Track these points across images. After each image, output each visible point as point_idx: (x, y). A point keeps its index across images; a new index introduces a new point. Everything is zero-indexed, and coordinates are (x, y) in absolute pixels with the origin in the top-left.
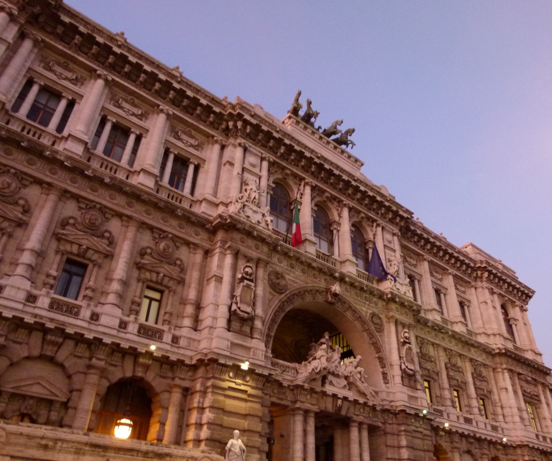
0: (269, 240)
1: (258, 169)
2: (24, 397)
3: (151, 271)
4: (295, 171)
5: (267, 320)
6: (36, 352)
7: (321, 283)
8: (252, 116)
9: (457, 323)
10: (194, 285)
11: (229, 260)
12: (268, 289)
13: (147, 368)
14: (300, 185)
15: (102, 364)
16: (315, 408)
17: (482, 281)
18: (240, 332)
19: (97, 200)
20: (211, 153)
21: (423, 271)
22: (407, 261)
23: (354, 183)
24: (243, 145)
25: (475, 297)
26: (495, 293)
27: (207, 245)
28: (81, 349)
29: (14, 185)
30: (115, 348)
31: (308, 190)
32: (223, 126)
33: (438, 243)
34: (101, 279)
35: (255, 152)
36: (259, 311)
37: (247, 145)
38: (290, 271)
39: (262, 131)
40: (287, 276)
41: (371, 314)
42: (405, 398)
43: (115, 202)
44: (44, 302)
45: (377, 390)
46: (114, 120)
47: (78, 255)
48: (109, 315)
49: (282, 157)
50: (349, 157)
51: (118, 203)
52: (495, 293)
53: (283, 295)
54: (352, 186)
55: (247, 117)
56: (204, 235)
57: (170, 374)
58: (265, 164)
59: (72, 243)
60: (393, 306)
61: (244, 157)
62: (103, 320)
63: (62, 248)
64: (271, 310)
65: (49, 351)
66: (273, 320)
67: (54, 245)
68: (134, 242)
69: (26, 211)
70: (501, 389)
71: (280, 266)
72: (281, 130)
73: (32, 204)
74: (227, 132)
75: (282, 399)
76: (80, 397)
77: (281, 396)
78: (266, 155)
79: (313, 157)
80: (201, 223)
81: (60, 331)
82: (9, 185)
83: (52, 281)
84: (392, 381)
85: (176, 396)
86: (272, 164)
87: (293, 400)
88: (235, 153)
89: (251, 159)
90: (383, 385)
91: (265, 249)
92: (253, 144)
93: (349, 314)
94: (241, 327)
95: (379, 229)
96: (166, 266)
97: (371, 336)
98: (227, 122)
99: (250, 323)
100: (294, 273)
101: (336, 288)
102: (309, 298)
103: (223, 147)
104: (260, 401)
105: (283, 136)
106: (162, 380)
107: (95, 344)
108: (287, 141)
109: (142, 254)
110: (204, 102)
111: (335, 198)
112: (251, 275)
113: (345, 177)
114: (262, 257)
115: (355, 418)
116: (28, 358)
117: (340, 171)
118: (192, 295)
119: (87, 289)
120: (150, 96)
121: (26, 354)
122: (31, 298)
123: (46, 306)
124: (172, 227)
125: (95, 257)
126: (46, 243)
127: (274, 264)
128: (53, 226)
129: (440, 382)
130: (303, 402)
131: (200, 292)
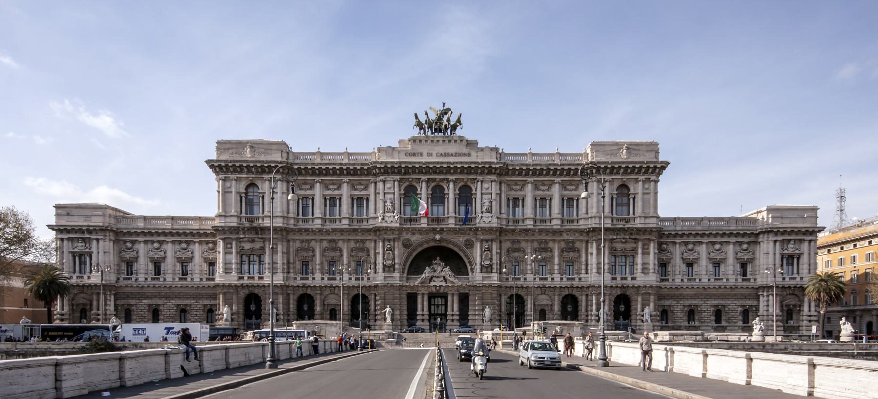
7: (431, 236)
10: (372, 256)
11: (381, 244)
18: (389, 272)
27: (374, 238)
30: (349, 287)
31: (424, 185)
36: (396, 261)
49: (405, 174)
50: (456, 141)
58: (396, 183)
66: (406, 262)
69: (313, 251)
71: (413, 231)
74: (375, 175)
85: (373, 297)
86: (400, 181)
88: (380, 185)
89: (388, 185)
93: (451, 246)
95: (479, 183)
97: (464, 253)
101: (438, 237)
102: (425, 246)
103: (376, 183)
109: (352, 251)
118: (372, 261)
122: (323, 279)
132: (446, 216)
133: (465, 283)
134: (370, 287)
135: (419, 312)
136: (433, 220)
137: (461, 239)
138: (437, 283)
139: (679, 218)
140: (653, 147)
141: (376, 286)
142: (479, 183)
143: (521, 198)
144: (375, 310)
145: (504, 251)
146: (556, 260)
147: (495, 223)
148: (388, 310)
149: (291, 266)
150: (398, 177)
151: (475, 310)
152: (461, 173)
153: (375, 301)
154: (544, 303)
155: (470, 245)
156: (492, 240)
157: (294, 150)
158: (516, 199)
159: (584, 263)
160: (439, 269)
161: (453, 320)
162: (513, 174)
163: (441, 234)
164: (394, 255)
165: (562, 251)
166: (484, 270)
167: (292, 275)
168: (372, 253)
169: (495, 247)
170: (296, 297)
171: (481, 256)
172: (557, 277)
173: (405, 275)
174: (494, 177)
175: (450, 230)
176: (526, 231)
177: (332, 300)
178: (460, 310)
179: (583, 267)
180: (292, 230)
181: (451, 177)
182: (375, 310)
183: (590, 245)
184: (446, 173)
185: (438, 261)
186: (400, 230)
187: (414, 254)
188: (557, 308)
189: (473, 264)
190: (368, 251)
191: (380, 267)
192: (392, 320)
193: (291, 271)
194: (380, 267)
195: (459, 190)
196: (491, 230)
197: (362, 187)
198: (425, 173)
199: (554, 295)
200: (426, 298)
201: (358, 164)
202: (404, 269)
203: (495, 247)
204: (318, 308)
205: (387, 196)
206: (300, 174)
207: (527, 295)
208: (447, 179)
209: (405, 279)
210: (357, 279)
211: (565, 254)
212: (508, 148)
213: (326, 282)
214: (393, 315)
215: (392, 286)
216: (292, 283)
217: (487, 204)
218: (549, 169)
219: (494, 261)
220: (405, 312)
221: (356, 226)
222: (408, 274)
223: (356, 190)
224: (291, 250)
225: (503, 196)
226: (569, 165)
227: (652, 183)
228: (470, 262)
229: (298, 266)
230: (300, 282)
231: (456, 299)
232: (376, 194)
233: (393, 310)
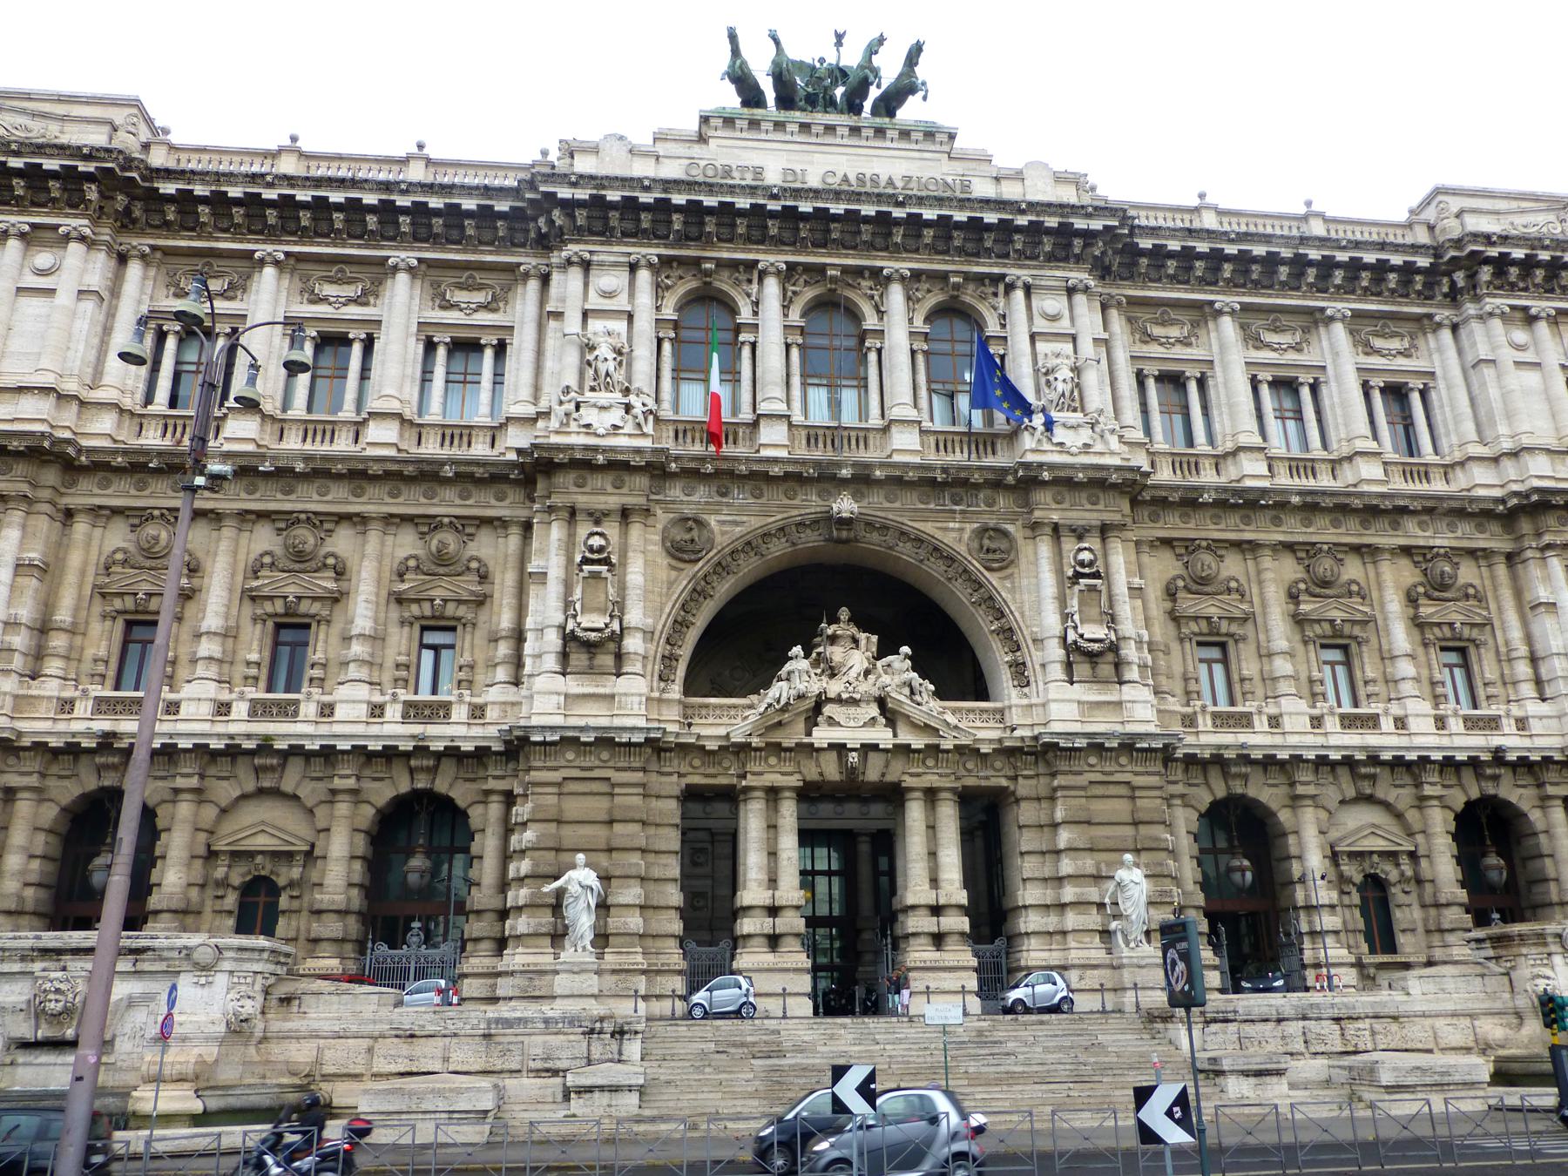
0: (637, 461)
1: (624, 297)
2: (251, 855)
3: (418, 601)
4: (725, 255)
5: (660, 627)
6: (250, 786)
7: (810, 503)
8: (574, 185)
9: (1350, 459)
11: (557, 532)
12: (664, 561)
13: (433, 771)
14: (750, 281)
15: (351, 783)
16: (794, 781)
17: (1477, 299)
18: (591, 671)
19: (299, 507)
20: (523, 306)
21: (1215, 348)
22: (1154, 339)
23: (898, 213)
24: (575, 259)
25: (1452, 353)
26: (1536, 318)
27: (522, 513)
28: (317, 768)
29: (164, 535)
31: (772, 287)
32: (533, 235)
33: (1259, 250)
34: (334, 639)
35: (612, 259)
36: (635, 615)
37: (587, 256)
38: (719, 503)
39: (613, 206)
40: (712, 520)
41: (973, 531)
42: (1072, 711)
43: (329, 498)
44: (240, 710)
45: (999, 705)
46: (314, 334)
47: (286, 615)
48: (347, 701)
49: (684, 239)
50: (905, 134)
51: (338, 498)
52: (1536, 318)
53: (700, 564)
54: (897, 222)
55: (564, 193)
56: (514, 495)
58: (644, 276)
59: (271, 598)
60: (1043, 497)
61: (586, 285)
62: (340, 712)
63: (259, 612)
64: (670, 604)
65: (266, 783)
66: (680, 625)
67: (248, 610)
68: (380, 559)
70: (1532, 608)
72: (654, 180)
73: (200, 555)
74: (545, 243)
75: (714, 776)
76: (328, 839)
77: (711, 771)
78: (639, 251)
79: (761, 202)
80: (493, 477)
81: (265, 746)
82: (156, 539)
83: (253, 671)
84: (1040, 678)
85: (495, 809)
87: (741, 772)
88: (567, 285)
90: (1014, 693)
91: (642, 481)
92: (602, 243)
93: (905, 552)
94: (590, 659)
95: (1019, 295)
96: (445, 582)
98: (535, 220)
99: (612, 646)
100: (728, 505)
101: (845, 505)
103: (545, 280)
104: (641, 790)
105: (665, 191)
106: (468, 785)
107: (328, 754)
108: (679, 199)
110: (469, 204)
111: (859, 272)
112: (601, 549)
113: (868, 210)
114: (630, 501)
115: (909, 781)
116: (244, 797)
117: (849, 201)
118: (506, 621)
119: (312, 666)
120: (367, 247)
121: (237, 793)
122: (223, 708)
123: (245, 716)
124: (448, 504)
125: (315, 608)
126: (234, 611)
127: (673, 502)
128: (240, 578)
129: (1262, 637)
130: (761, 774)
131: (521, 610)
132: (875, 421)
133: (986, 733)
134: (481, 754)
135: (752, 893)
136: (813, 435)
137: (954, 532)
138: (852, 728)
141: (517, 747)
142: (1019, 295)
143: (1192, 372)
144: (504, 886)
145: (1155, 593)
146: (1400, 637)
147: (1112, 454)
148: (581, 878)
149: (58, 642)
150: (653, 252)
151: (1060, 880)
152: (934, 250)
153: (508, 830)
154: (1379, 844)
155: (998, 550)
156: (1105, 530)
157: (175, 138)
158: (1173, 380)
159: (1523, 650)
160: (858, 660)
161: (938, 939)
162: (1156, 274)
163: (857, 496)
164: (622, 588)
165: (1412, 600)
166: (1082, 670)
167: (50, 688)
168: (504, 581)
169: (1119, 560)
170: (50, 813)
171: (1062, 600)
172: (1419, 711)
173: (676, 691)
174: (1078, 276)
175: (899, 481)
176: (1247, 503)
177: (264, 827)
178: (969, 882)
179: (1523, 669)
180: (101, 467)
181: (889, 265)
182: (504, 886)
183: (1534, 571)
184: (871, 246)
185: (844, 629)
186: (657, 470)
187: (724, 589)
188: (1445, 868)
189: (1024, 635)
190: (484, 577)
191: (543, 646)
192: (602, 939)
193: (53, 666)
194: (543, 646)
195: (928, 319)
196: (1098, 483)
197: (480, 297)
198: (778, 243)
199: (1421, 801)
200: (789, 812)
201: (469, 190)
202: (669, 660)
203: (1119, 560)
204: (173, 878)
205: (595, 325)
206: (189, 223)
207: (1295, 801)
208: (876, 273)
209: (674, 713)
210: (413, 711)
211: (1427, 610)
212: (1115, 187)
213: (240, 725)
214: (603, 907)
215: (605, 741)
216: (39, 726)
217: (1065, 373)
218: (1300, 263)
219: (1128, 627)
220: (674, 896)
221: (432, 448)
222: (687, 691)
223: (449, 306)
224: (75, 559)
225: (1121, 356)
226: (1382, 246)
228: (1008, 634)
229: (102, 640)
230: (85, 724)
231: (948, 815)
232: (548, 315)
233: (605, 878)
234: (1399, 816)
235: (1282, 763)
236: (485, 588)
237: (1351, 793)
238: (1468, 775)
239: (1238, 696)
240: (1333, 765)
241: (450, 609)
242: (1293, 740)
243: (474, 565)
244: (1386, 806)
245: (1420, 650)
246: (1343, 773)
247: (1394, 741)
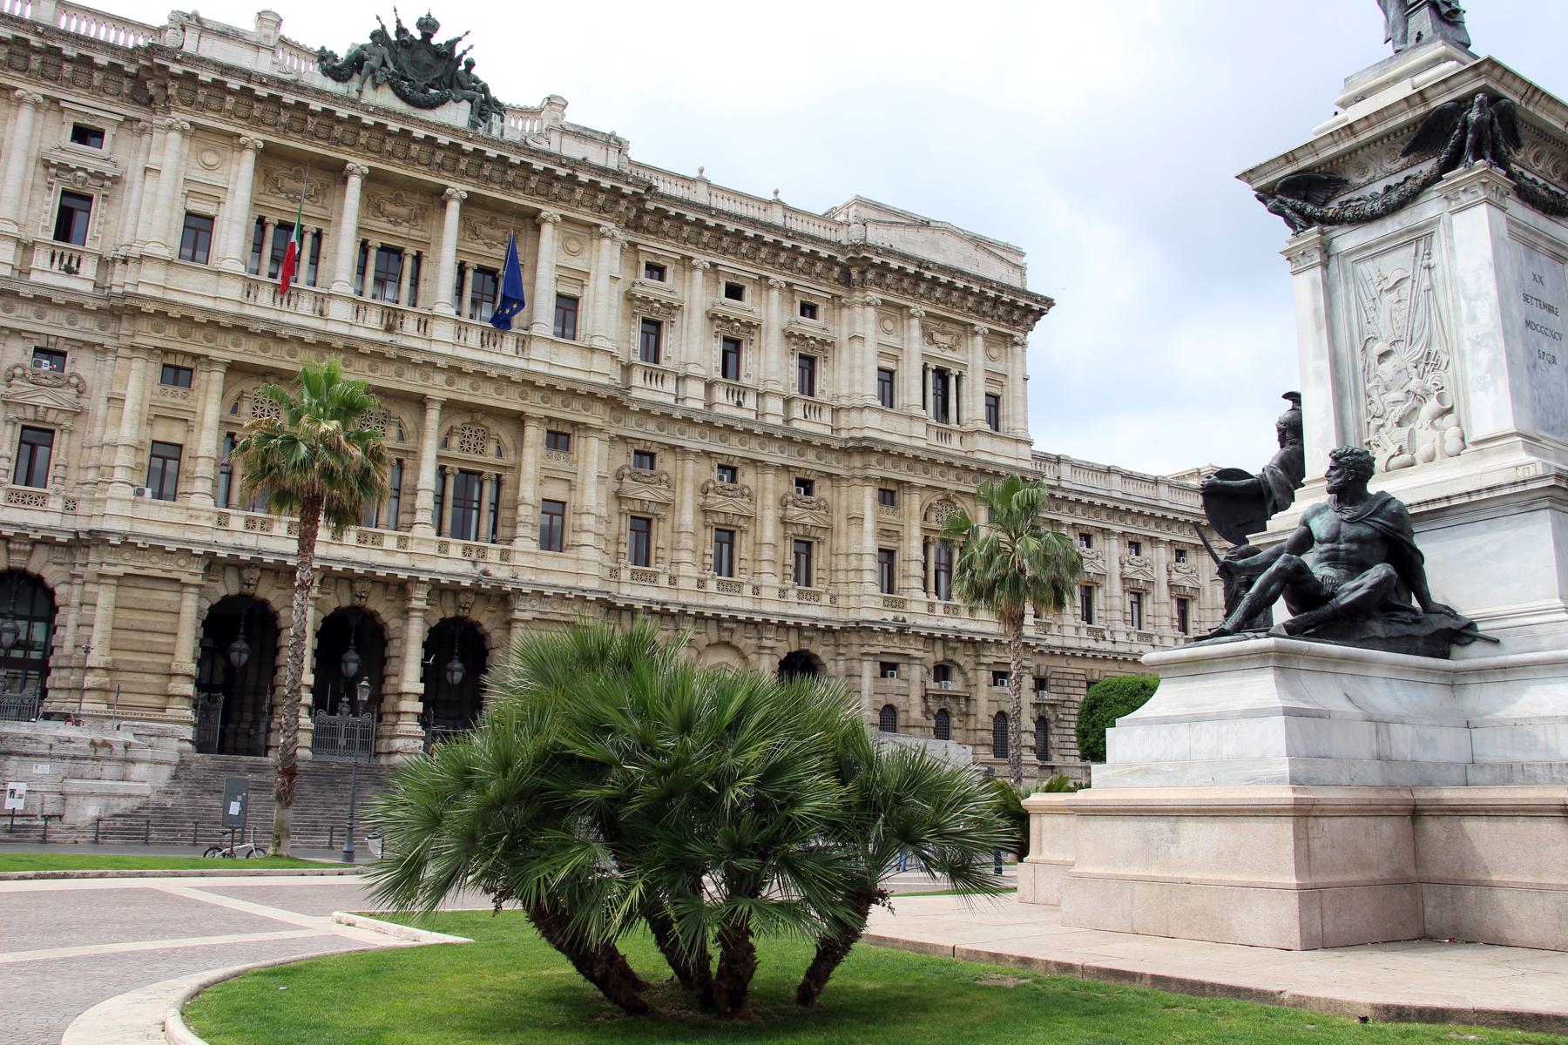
13: (30, 554)
57: (67, 559)
139: (1068, 461)
140: (1010, 255)
211: (793, 512)
227: (1019, 349)
234: (744, 658)
235: (673, 615)
236: (84, 402)
237: (714, 639)
238: (793, 636)
239: (653, 560)
240: (707, 619)
241: (51, 416)
242: (683, 599)
243: (74, 380)
244: (737, 649)
245: (781, 542)
246: (712, 625)
247: (748, 605)
